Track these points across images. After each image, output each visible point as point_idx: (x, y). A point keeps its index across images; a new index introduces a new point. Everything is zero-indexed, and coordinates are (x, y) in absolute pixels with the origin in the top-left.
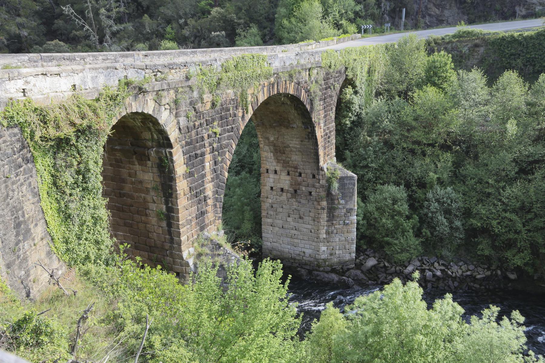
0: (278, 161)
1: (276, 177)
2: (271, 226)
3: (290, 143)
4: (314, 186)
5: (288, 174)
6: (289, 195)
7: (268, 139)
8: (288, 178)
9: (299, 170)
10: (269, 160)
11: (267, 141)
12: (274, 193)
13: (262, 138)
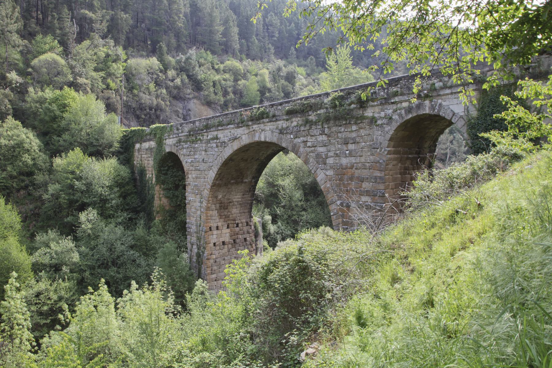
0: (221, 216)
1: (219, 232)
2: (215, 281)
3: (234, 198)
4: (248, 233)
5: (228, 227)
6: (230, 246)
7: (216, 197)
8: (228, 231)
9: (237, 222)
10: (213, 218)
11: (215, 200)
12: (218, 248)
13: (211, 197)
